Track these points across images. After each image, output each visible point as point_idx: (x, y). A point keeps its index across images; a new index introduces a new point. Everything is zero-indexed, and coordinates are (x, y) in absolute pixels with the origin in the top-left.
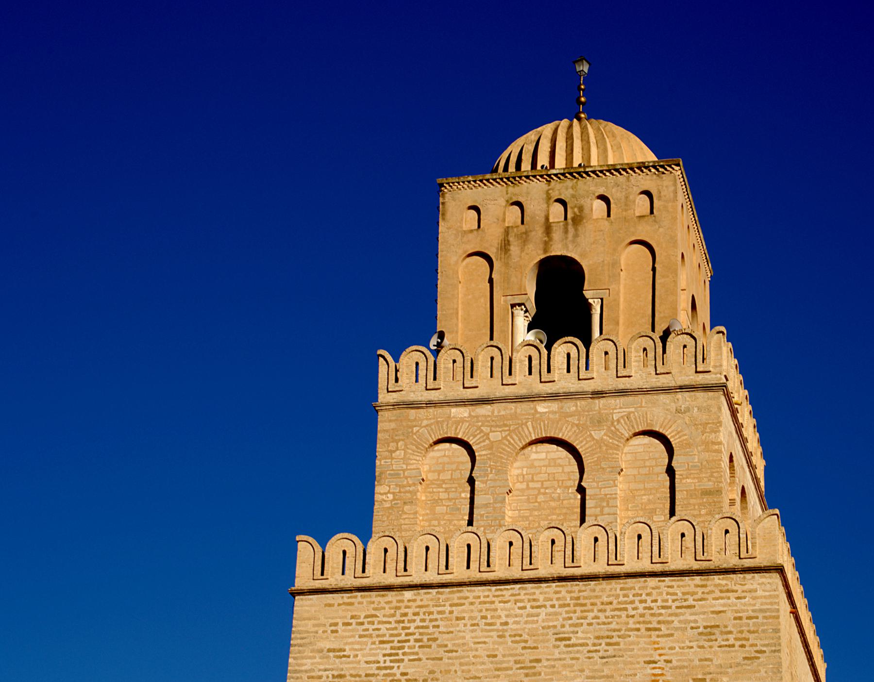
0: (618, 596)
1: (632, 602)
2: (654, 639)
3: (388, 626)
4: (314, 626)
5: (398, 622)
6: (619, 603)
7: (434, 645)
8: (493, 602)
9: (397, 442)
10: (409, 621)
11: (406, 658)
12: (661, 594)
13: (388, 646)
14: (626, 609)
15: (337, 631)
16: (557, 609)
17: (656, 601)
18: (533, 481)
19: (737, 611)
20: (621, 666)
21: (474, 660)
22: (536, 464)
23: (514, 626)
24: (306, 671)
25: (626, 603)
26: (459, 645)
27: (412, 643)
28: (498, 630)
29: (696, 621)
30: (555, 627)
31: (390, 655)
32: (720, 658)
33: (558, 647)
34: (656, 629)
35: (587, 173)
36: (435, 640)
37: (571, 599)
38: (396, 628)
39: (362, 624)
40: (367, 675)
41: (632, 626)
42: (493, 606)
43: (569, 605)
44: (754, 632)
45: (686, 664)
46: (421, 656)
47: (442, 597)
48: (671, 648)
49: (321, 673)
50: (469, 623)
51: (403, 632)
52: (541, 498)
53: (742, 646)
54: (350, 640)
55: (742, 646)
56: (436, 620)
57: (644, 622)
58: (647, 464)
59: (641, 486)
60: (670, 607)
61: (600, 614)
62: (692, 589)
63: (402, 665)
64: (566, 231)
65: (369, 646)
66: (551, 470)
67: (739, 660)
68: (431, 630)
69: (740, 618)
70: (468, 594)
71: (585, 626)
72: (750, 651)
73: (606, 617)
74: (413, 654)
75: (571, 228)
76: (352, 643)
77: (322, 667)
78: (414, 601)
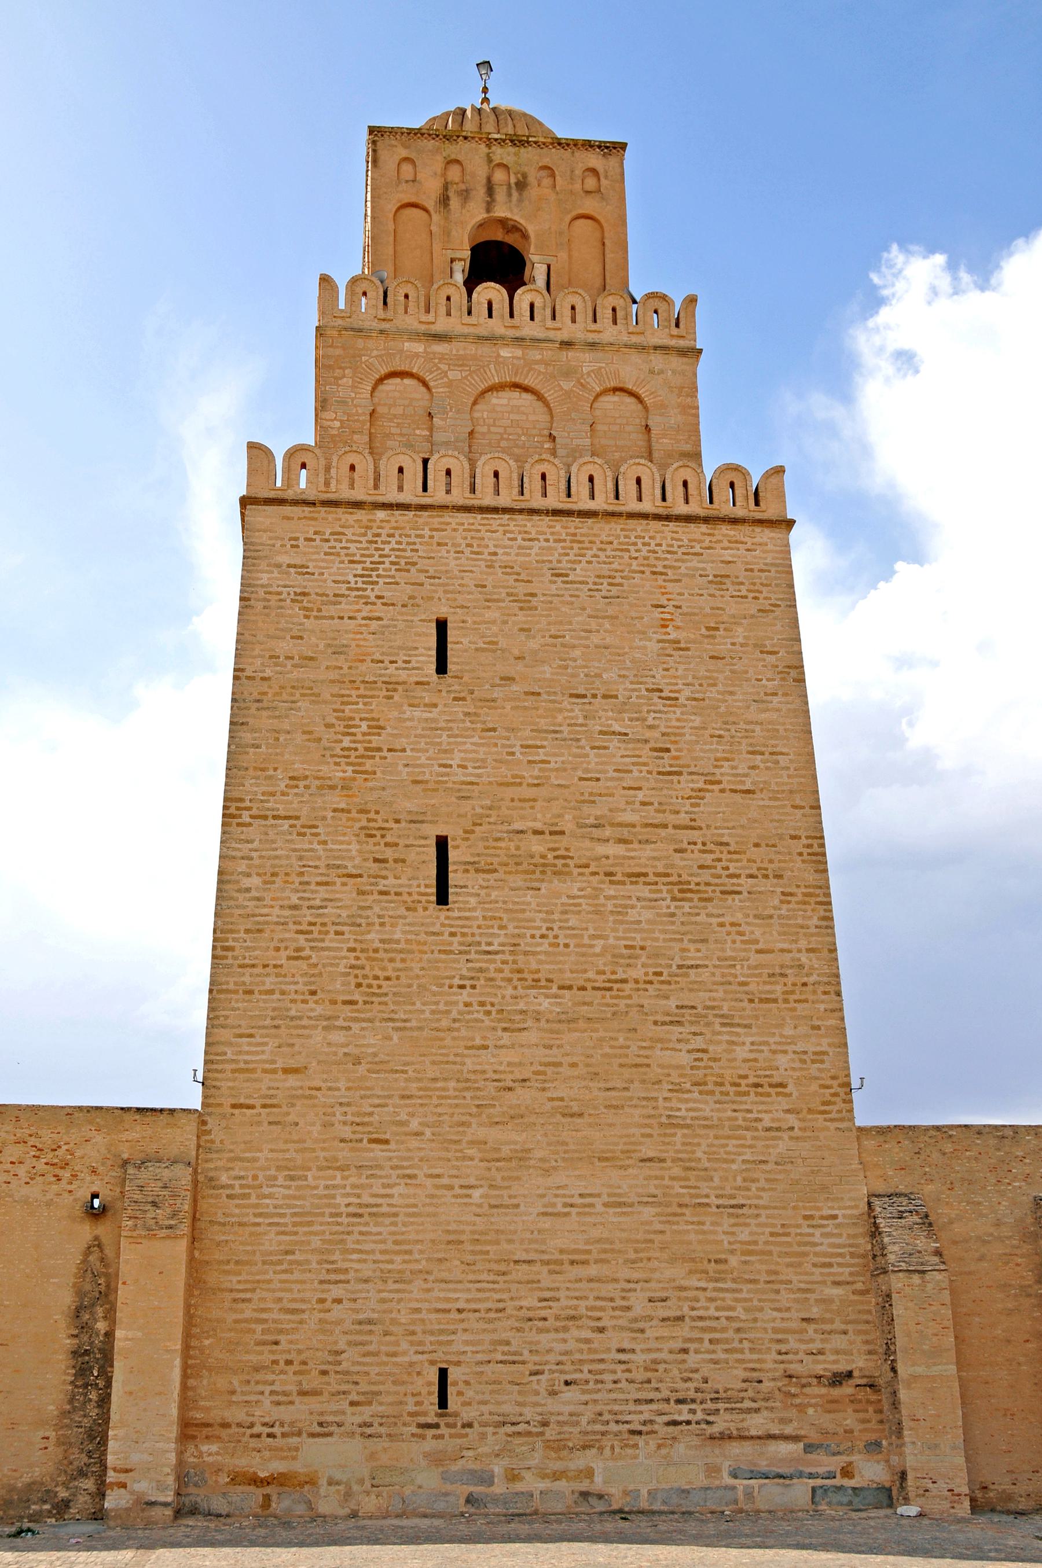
0: (618, 537)
1: (635, 544)
2: (660, 583)
3: (359, 545)
4: (270, 538)
5: (371, 542)
6: (620, 544)
7: (413, 570)
8: (479, 531)
9: (344, 369)
10: (383, 543)
11: (381, 581)
12: (665, 538)
13: (360, 566)
14: (628, 551)
15: (297, 546)
16: (551, 544)
17: (660, 545)
18: (494, 425)
19: (747, 563)
20: (626, 607)
21: (460, 589)
22: (498, 409)
23: (505, 558)
24: (262, 586)
25: (628, 544)
26: (441, 572)
27: (387, 565)
28: (486, 560)
29: (704, 569)
30: (550, 562)
31: (362, 576)
32: (733, 608)
33: (555, 582)
34: (662, 574)
35: (528, 142)
36: (414, 564)
37: (567, 534)
38: (367, 549)
39: (327, 541)
40: (335, 595)
41: (634, 567)
42: (479, 535)
43: (565, 541)
44: (767, 585)
45: (696, 611)
46: (398, 580)
47: (421, 521)
48: (680, 594)
49: (280, 589)
50: (453, 550)
51: (377, 554)
52: (504, 444)
53: (755, 598)
54: (314, 557)
55: (755, 598)
56: (414, 543)
57: (648, 565)
58: (618, 421)
59: (612, 442)
60: (676, 553)
61: (600, 553)
62: (697, 536)
63: (376, 587)
64: (510, 195)
65: (337, 565)
66: (512, 416)
67: (753, 611)
68: (408, 554)
69: (752, 570)
70: (449, 520)
71: (584, 564)
72: (765, 604)
73: (608, 557)
74: (389, 577)
75: (515, 194)
76: (316, 560)
77: (281, 583)
78: (388, 521)
